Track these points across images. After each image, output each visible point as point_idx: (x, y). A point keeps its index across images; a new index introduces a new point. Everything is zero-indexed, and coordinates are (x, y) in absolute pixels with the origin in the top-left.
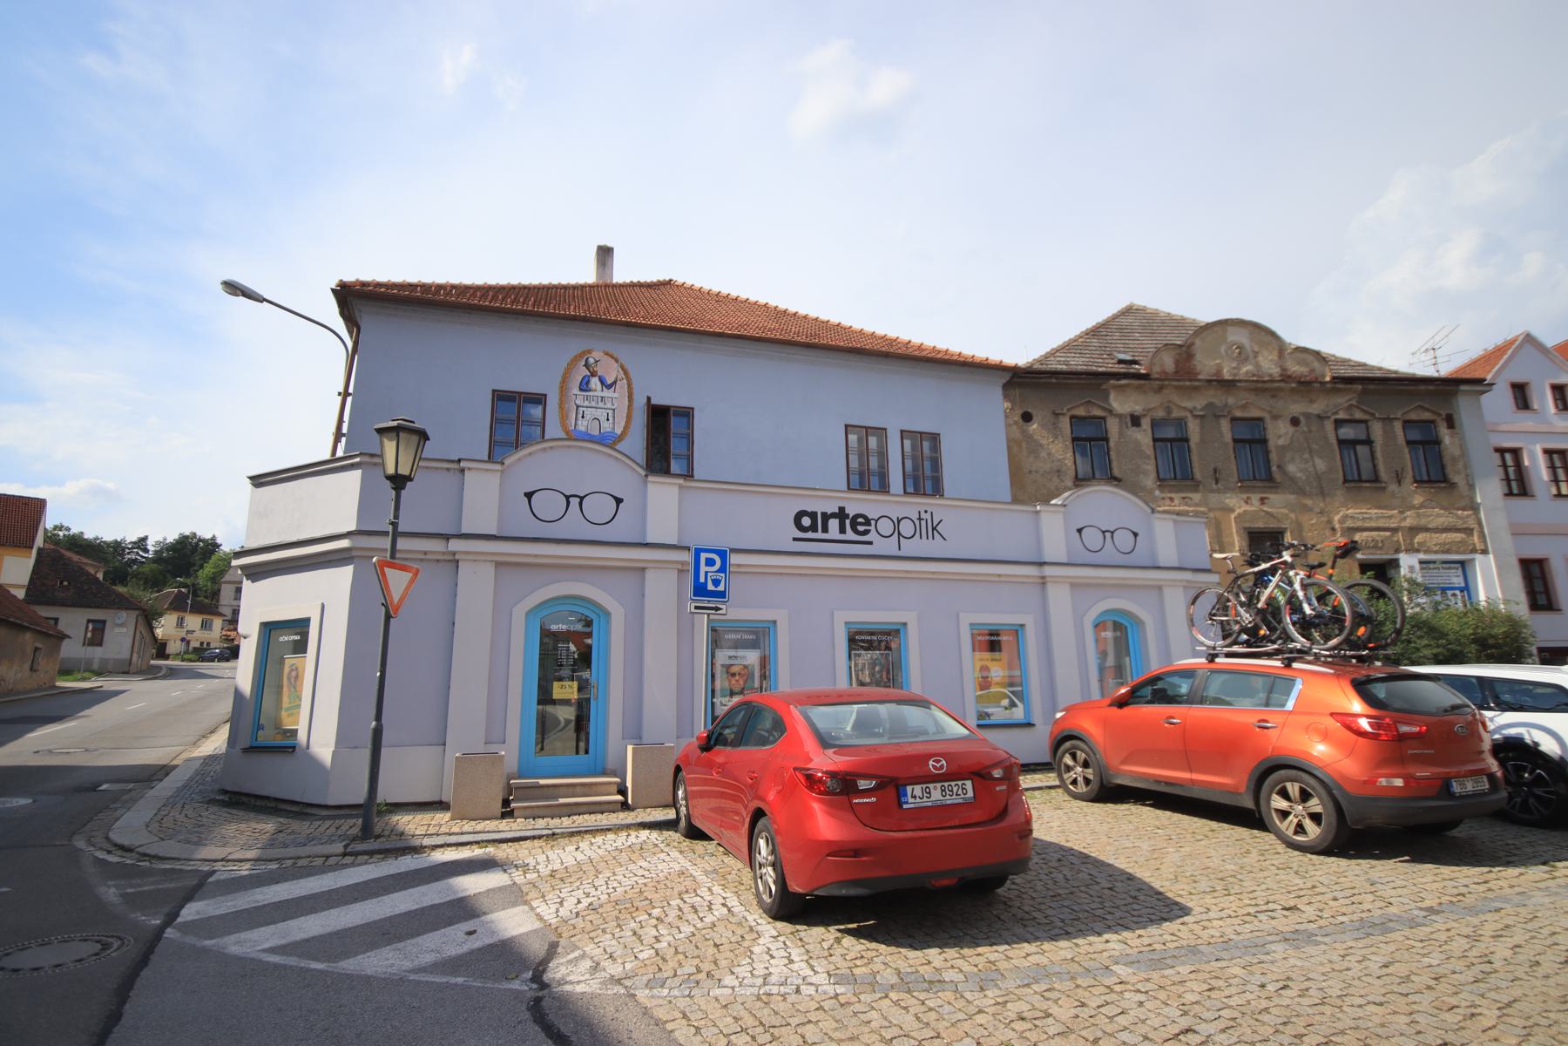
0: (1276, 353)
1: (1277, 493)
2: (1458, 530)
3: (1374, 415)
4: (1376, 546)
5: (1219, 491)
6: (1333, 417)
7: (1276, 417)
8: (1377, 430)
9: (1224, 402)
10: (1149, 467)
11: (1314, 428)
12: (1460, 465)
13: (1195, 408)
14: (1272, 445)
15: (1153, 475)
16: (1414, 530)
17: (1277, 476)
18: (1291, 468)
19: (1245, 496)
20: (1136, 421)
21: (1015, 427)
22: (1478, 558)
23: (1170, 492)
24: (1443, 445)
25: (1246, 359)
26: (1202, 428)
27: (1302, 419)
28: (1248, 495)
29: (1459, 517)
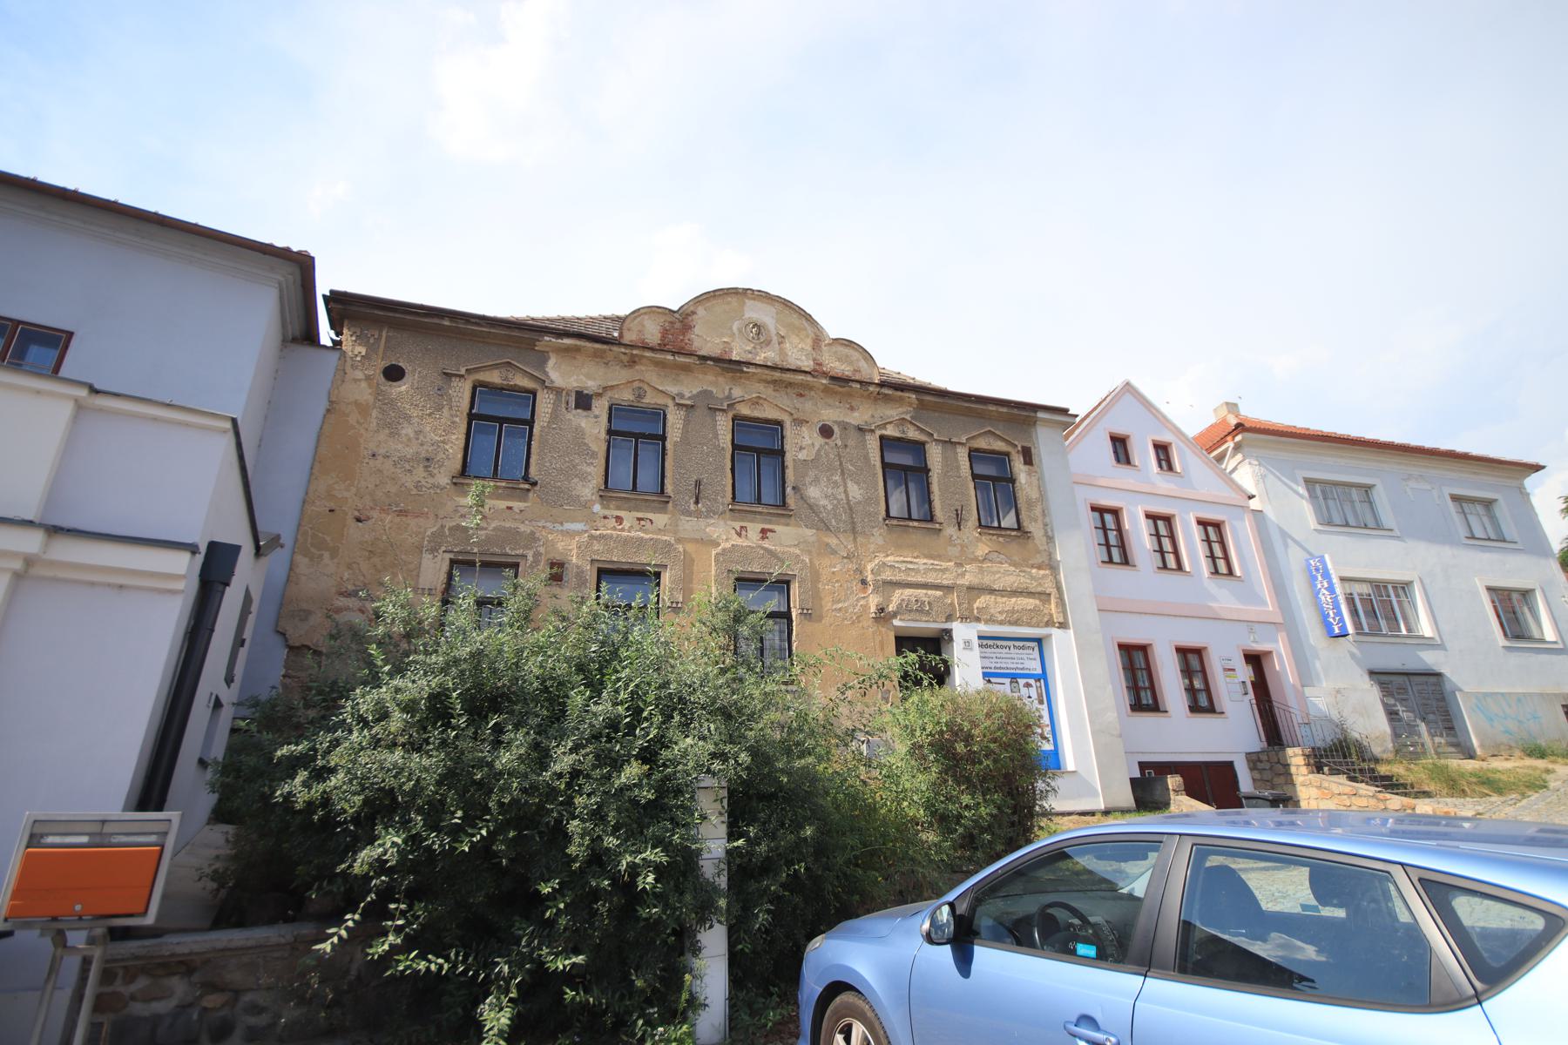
0: (809, 341)
1: (788, 525)
2: (1031, 594)
3: (932, 435)
4: (920, 610)
5: (698, 515)
6: (878, 433)
7: (799, 422)
8: (935, 455)
9: (727, 393)
10: (590, 469)
11: (851, 443)
12: (1038, 511)
13: (681, 396)
14: (789, 458)
15: (596, 479)
16: (975, 590)
17: (791, 500)
18: (813, 492)
19: (737, 525)
20: (583, 401)
21: (364, 385)
22: (1056, 633)
23: (618, 508)
24: (1017, 484)
25: (768, 343)
26: (687, 422)
27: (836, 429)
28: (743, 524)
29: (1032, 578)
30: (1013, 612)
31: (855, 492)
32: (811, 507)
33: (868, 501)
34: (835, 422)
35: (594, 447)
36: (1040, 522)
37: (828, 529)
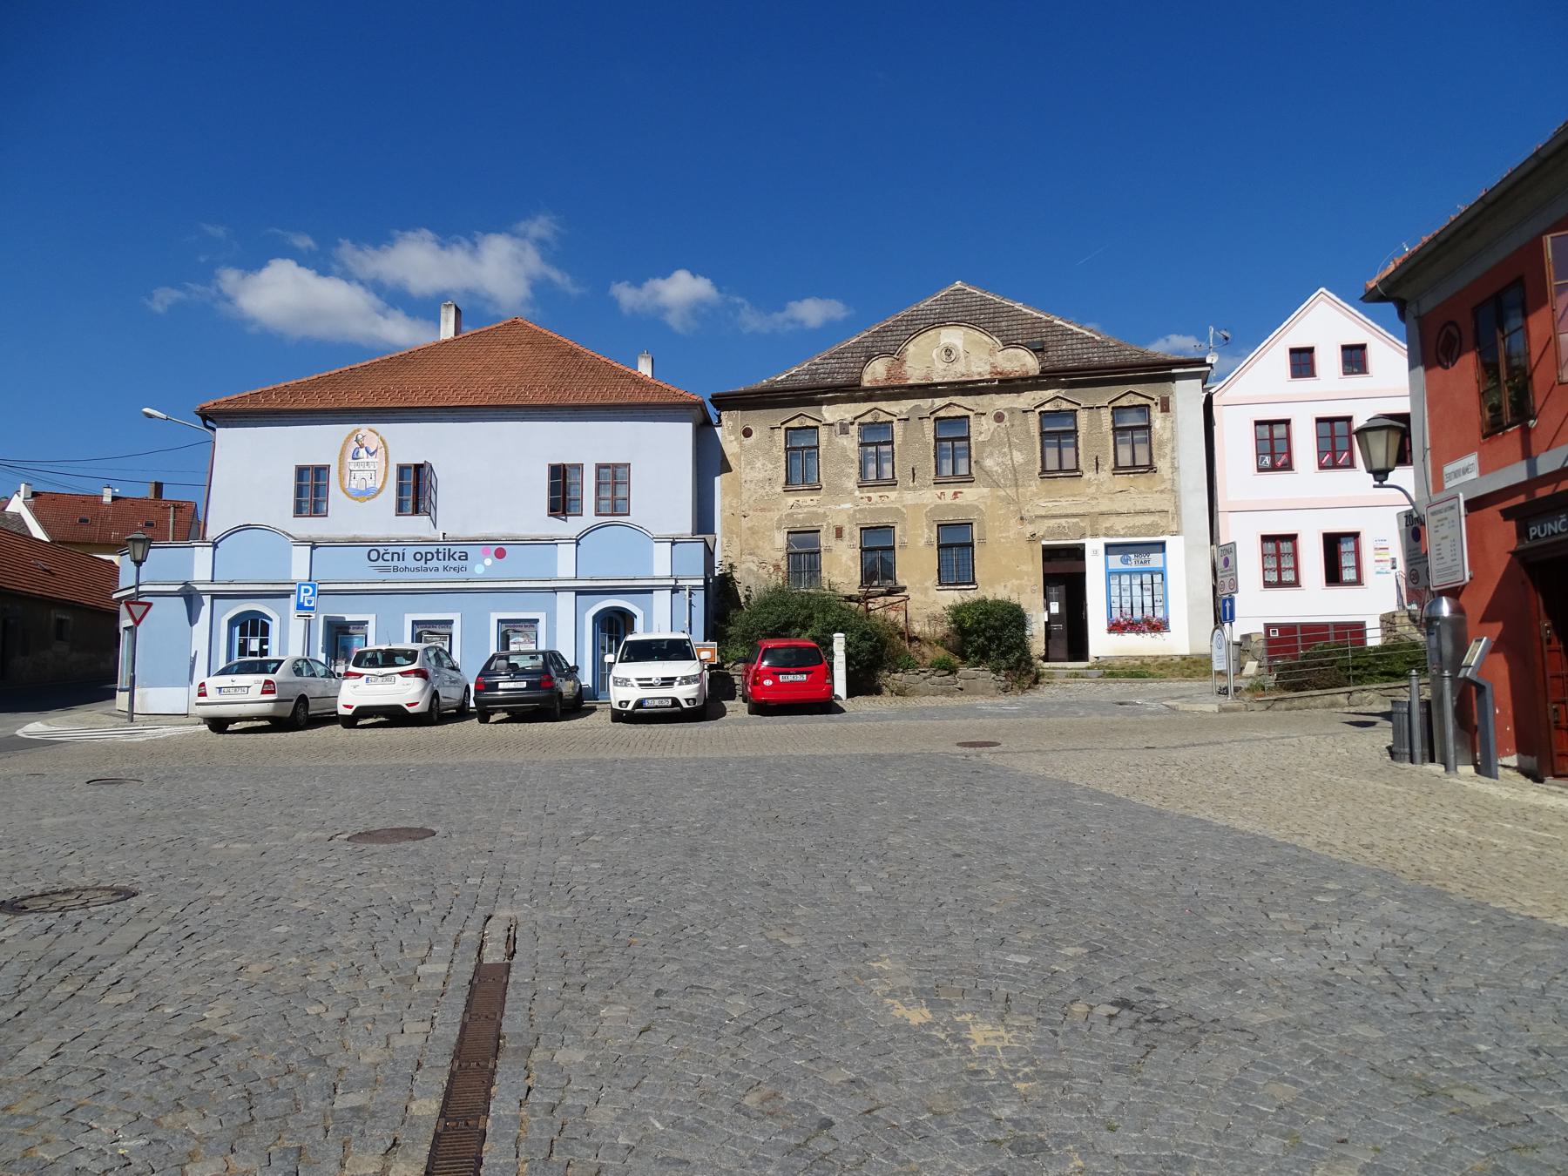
4: (1060, 532)
5: (915, 489)
6: (1038, 410)
8: (1083, 418)
10: (851, 471)
11: (1016, 422)
12: (1167, 450)
13: (901, 412)
18: (989, 463)
19: (938, 492)
20: (844, 430)
21: (735, 443)
23: (869, 492)
26: (905, 429)
27: (1006, 414)
30: (1134, 527)
31: (1018, 457)
32: (987, 473)
33: (1027, 463)
34: (1005, 410)
35: (852, 457)
36: (1168, 457)
37: (999, 486)
